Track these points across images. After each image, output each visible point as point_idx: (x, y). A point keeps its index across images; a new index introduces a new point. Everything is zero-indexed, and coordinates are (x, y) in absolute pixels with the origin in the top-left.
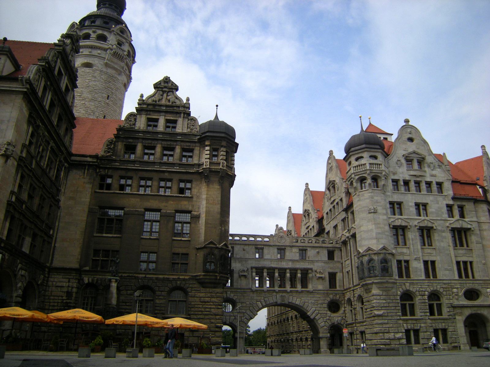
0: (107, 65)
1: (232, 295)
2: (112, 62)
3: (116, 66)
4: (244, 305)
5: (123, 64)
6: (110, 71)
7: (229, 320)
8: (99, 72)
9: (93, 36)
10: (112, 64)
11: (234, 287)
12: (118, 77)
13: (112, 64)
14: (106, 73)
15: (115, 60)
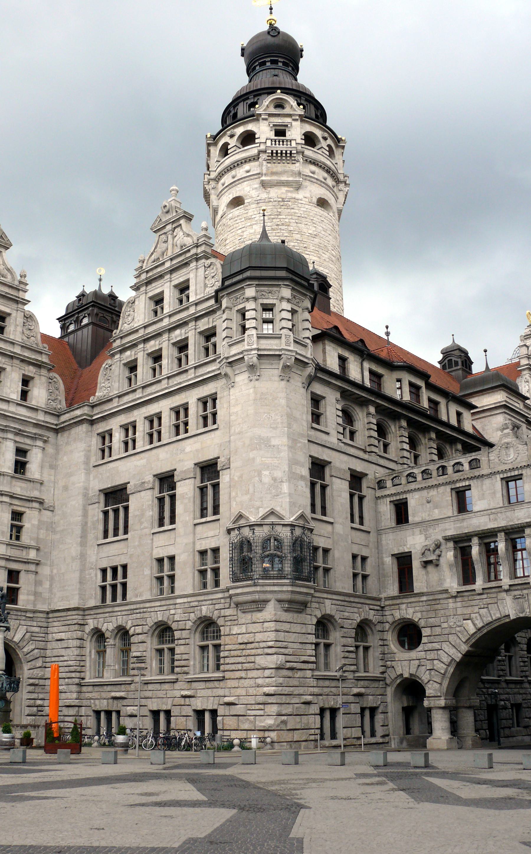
0: (264, 185)
1: (411, 611)
2: (273, 173)
3: (284, 178)
4: (437, 630)
5: (297, 167)
6: (275, 193)
7: (407, 670)
8: (254, 206)
9: (233, 142)
10: (275, 178)
11: (415, 592)
12: (294, 195)
13: (275, 178)
14: (268, 201)
15: (279, 167)
